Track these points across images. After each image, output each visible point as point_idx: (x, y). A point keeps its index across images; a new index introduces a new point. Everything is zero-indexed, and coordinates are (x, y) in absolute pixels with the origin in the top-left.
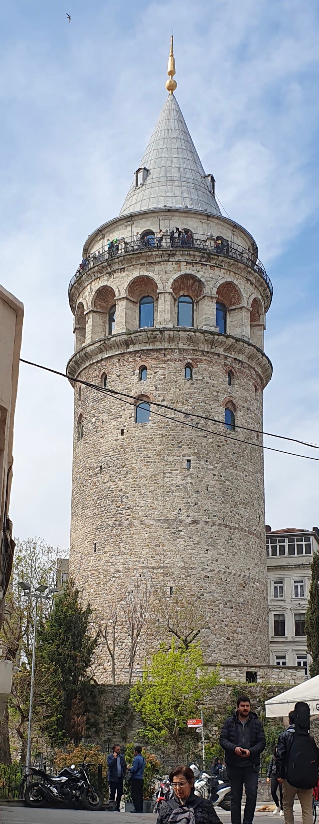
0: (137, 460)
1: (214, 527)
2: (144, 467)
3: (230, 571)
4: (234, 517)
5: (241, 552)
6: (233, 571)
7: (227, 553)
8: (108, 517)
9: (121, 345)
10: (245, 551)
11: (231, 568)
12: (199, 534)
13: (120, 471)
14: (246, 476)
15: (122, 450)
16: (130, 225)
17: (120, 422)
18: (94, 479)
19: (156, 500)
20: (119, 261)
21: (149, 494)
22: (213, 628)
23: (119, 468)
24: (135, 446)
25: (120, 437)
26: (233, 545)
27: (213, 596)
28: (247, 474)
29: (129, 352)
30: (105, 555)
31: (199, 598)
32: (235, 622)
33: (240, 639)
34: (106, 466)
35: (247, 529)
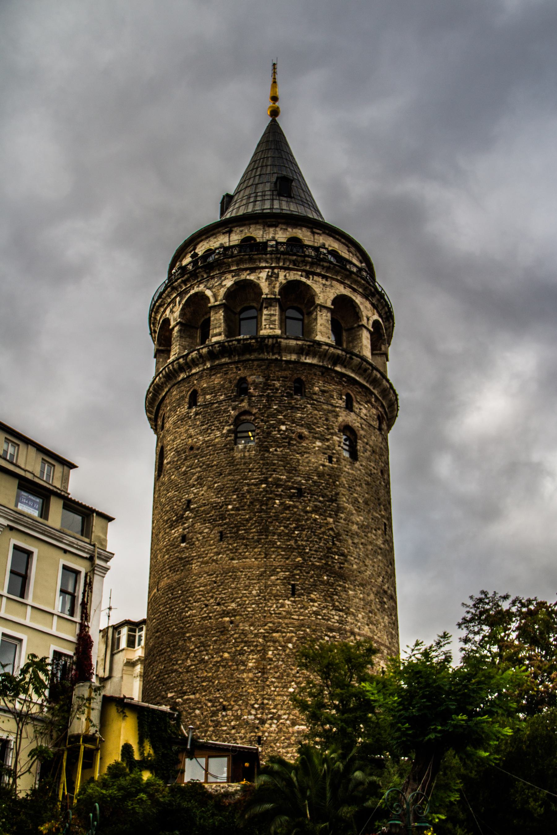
0: (348, 500)
2: (354, 512)
8: (315, 556)
9: (329, 359)
13: (330, 505)
15: (331, 480)
16: (318, 234)
17: (328, 446)
18: (287, 502)
19: (367, 556)
20: (326, 267)
21: (361, 546)
23: (327, 501)
24: (345, 482)
25: (327, 464)
29: (337, 372)
30: (311, 604)
34: (307, 491)
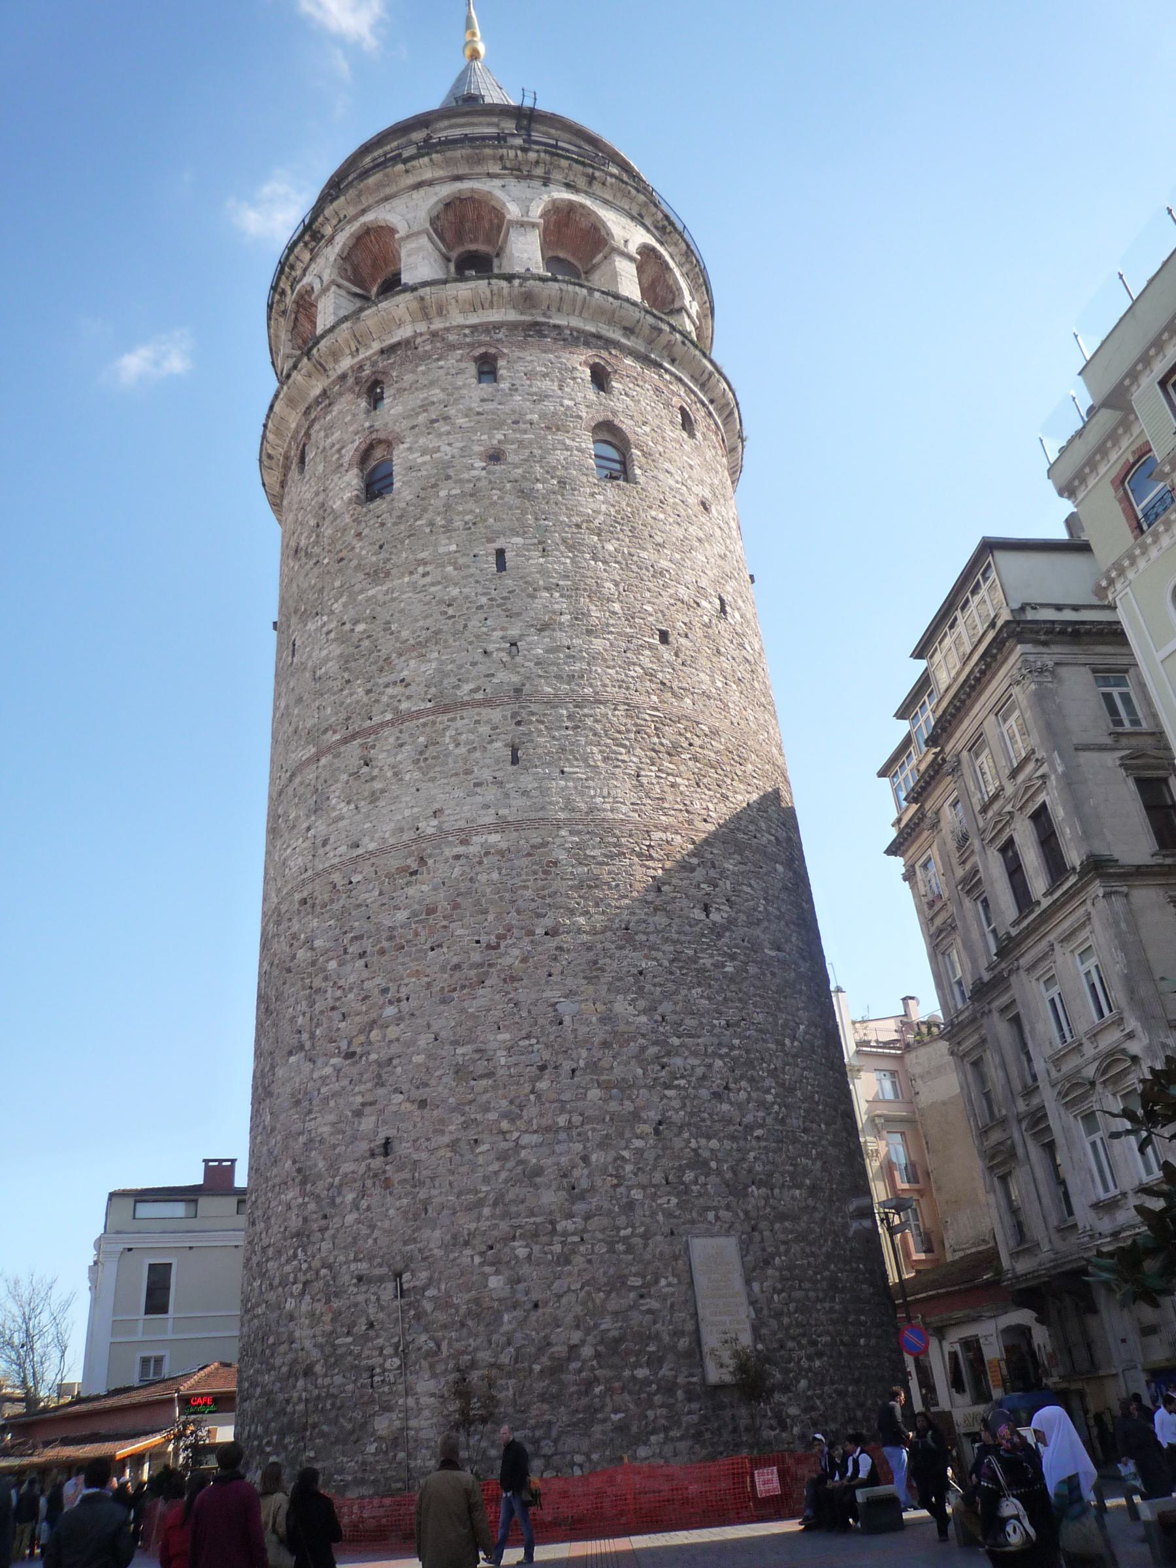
1: (323, 761)
3: (360, 851)
4: (377, 701)
5: (401, 779)
6: (372, 846)
7: (352, 806)
10: (420, 768)
11: (366, 840)
12: (296, 800)
14: (424, 575)
22: (308, 1045)
26: (376, 772)
27: (312, 949)
28: (428, 568)
31: (289, 971)
32: (376, 991)
33: (391, 1041)
35: (429, 705)
